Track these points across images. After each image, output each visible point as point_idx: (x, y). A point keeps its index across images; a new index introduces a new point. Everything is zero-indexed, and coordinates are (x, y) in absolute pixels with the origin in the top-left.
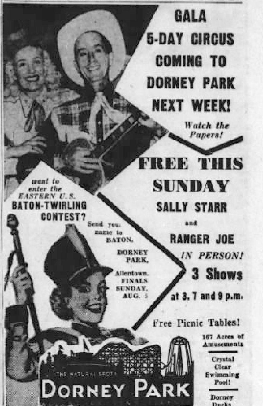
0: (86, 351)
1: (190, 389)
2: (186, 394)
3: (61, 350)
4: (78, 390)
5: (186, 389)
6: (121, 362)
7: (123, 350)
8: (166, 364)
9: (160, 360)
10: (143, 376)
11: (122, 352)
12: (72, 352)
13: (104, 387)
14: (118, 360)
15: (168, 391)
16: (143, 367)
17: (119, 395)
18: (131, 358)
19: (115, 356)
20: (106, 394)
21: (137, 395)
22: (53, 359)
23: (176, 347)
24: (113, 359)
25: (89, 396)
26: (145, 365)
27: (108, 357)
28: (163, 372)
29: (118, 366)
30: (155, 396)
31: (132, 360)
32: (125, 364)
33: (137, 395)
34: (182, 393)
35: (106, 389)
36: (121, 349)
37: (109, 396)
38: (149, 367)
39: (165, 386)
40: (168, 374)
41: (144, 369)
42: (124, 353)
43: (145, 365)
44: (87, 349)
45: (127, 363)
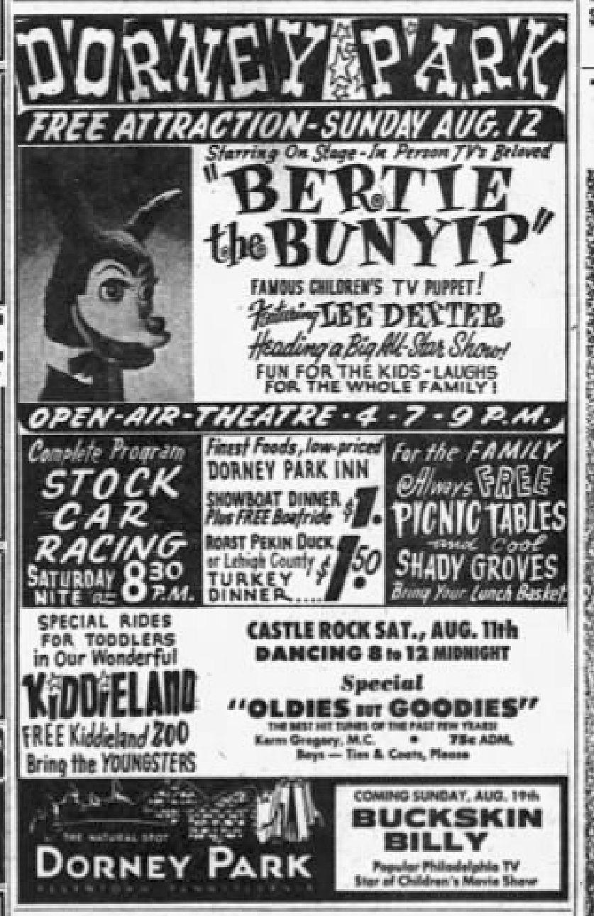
2: (305, 873)
4: (103, 864)
5: (305, 865)
6: (183, 817)
10: (226, 843)
13: (152, 859)
17: (180, 875)
20: (156, 872)
21: (212, 874)
25: (123, 875)
26: (228, 823)
27: (158, 808)
28: (262, 836)
29: (178, 824)
33: (212, 874)
34: (297, 873)
35: (155, 863)
36: (183, 795)
37: (161, 876)
38: (236, 825)
39: (265, 859)
40: (272, 838)
42: (189, 802)
43: (228, 823)
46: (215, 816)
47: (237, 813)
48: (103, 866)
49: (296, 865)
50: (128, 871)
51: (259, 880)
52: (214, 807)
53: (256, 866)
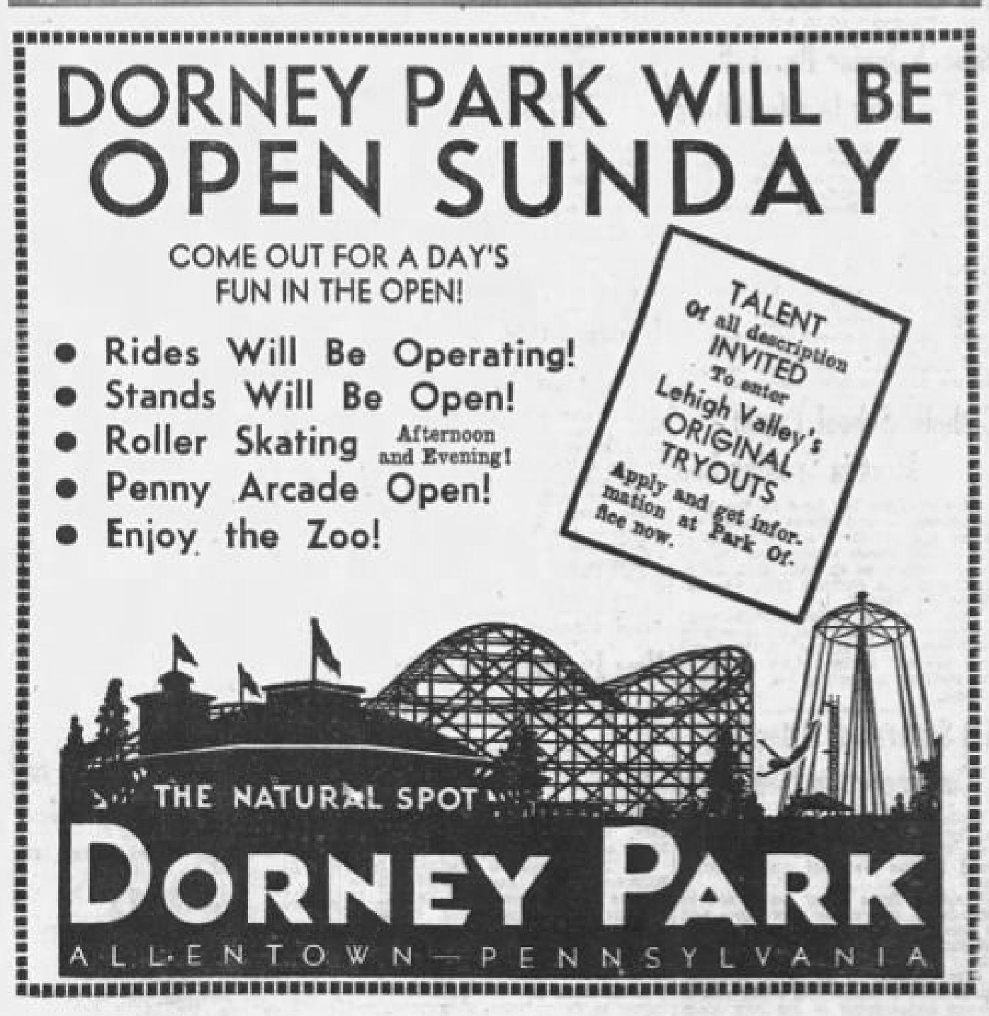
0: (324, 674)
1: (923, 888)
2: (904, 914)
3: (184, 667)
5: (901, 885)
6: (523, 741)
7: (538, 673)
8: (785, 753)
9: (750, 728)
10: (657, 815)
11: (532, 681)
12: (246, 681)
13: (424, 865)
14: (510, 725)
15: (796, 897)
16: (655, 766)
17: (513, 915)
18: (583, 719)
19: (488, 707)
20: (437, 904)
21: (613, 914)
22: (133, 717)
23: (844, 659)
24: (476, 718)
25: (338, 914)
30: (724, 922)
31: (589, 726)
32: (550, 749)
33: (613, 914)
34: (876, 905)
35: (438, 878)
36: (523, 670)
37: (458, 917)
39: (779, 866)
40: (798, 802)
41: (658, 775)
42: (539, 692)
43: (664, 754)
44: (334, 665)
45: (561, 742)
46: (623, 739)
47: (693, 727)
48: (276, 883)
49: (874, 884)
50: (354, 905)
51: (761, 931)
52: (621, 708)
53: (753, 896)
